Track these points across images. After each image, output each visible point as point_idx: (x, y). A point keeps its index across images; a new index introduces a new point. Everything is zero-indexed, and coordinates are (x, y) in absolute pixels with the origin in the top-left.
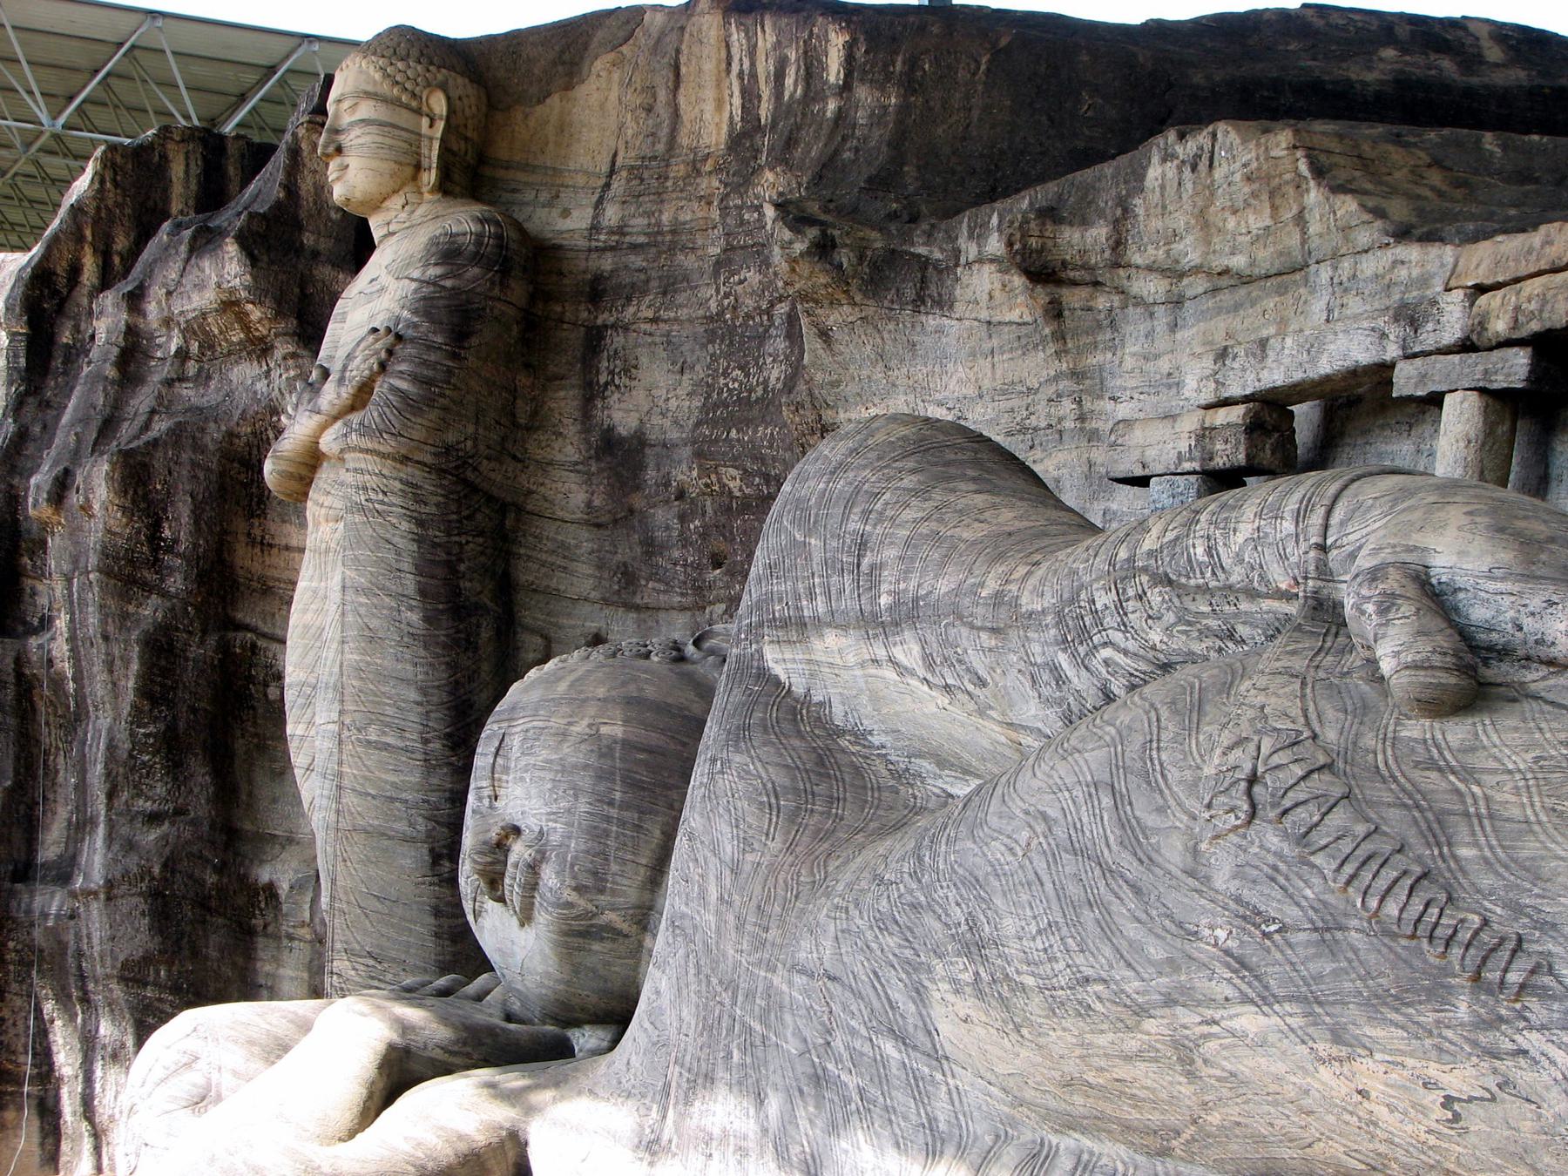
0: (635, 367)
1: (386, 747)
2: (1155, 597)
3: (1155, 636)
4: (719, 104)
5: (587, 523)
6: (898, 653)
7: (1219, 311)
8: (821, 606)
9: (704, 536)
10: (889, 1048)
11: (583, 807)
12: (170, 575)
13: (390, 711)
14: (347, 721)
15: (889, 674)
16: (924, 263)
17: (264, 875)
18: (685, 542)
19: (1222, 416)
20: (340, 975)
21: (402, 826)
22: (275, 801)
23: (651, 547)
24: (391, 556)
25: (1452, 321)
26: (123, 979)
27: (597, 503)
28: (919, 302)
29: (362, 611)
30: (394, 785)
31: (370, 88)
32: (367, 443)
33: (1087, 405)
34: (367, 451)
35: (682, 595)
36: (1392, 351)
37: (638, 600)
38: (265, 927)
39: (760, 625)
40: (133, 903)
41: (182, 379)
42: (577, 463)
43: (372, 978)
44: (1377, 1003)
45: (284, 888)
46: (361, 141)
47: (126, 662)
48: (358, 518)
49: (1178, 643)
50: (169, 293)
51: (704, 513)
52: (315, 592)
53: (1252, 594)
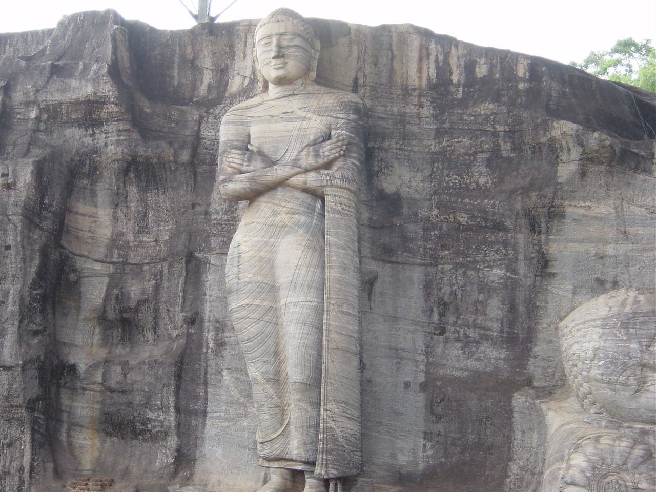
0: (391, 167)
1: (349, 314)
4: (420, 70)
5: (369, 226)
9: (439, 238)
12: (45, 221)
13: (350, 299)
14: (333, 302)
16: (637, 154)
17: (72, 361)
18: (426, 240)
20: (331, 411)
21: (353, 348)
22: (62, 327)
23: (405, 239)
24: (351, 233)
26: (27, 408)
27: (375, 218)
28: (636, 169)
29: (341, 255)
30: (351, 330)
31: (300, 33)
32: (346, 185)
34: (345, 188)
35: (421, 259)
37: (394, 259)
38: (65, 383)
40: (33, 372)
41: (39, 130)
42: (365, 201)
43: (344, 412)
45: (82, 367)
46: (295, 54)
47: (32, 259)
48: (337, 216)
50: (37, 91)
51: (441, 228)
52: (266, 243)
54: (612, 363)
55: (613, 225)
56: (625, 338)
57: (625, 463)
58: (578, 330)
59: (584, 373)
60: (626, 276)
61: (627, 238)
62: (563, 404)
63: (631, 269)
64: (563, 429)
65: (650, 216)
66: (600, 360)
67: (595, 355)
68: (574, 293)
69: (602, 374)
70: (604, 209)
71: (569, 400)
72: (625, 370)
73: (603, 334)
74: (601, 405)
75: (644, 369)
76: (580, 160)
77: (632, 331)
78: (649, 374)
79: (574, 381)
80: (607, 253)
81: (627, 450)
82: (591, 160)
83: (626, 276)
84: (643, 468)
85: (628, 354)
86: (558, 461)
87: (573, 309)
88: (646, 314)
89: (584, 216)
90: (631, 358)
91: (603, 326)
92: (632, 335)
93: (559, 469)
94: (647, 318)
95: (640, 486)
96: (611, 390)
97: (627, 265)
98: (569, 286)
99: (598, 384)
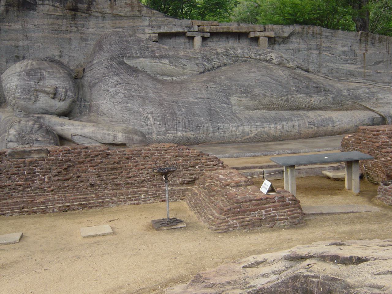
2: (225, 57)
3: (225, 61)
6: (163, 61)
7: (116, 20)
8: (139, 55)
10: (224, 105)
11: (71, 83)
15: (159, 64)
19: (154, 35)
25: (196, 28)
28: (29, 9)
33: (79, 28)
36: (186, 31)
39: (122, 57)
44: (314, 93)
49: (229, 61)
53: (242, 57)
54: (23, 90)
55: (21, 33)
56: (28, 80)
57: (31, 131)
58: (9, 78)
59: (13, 95)
60: (28, 54)
61: (28, 38)
62: (6, 110)
63: (30, 51)
64: (6, 119)
65: (36, 28)
66: (19, 89)
67: (16, 88)
68: (7, 63)
69: (20, 95)
70: (17, 26)
71: (8, 107)
72: (29, 93)
73: (19, 79)
74: (21, 108)
75: (37, 92)
76: (5, 5)
77: (31, 77)
78: (39, 94)
79: (9, 99)
80: (20, 45)
81: (32, 125)
82: (10, 5)
83: (28, 54)
84: (39, 132)
85: (30, 86)
86: (4, 133)
87: (6, 69)
88: (36, 69)
89: (9, 29)
90: (31, 88)
91: (19, 75)
92: (31, 78)
93: (5, 136)
94: (36, 71)
95: (38, 139)
96: (24, 101)
97: (28, 50)
98: (4, 60)
99: (19, 100)
